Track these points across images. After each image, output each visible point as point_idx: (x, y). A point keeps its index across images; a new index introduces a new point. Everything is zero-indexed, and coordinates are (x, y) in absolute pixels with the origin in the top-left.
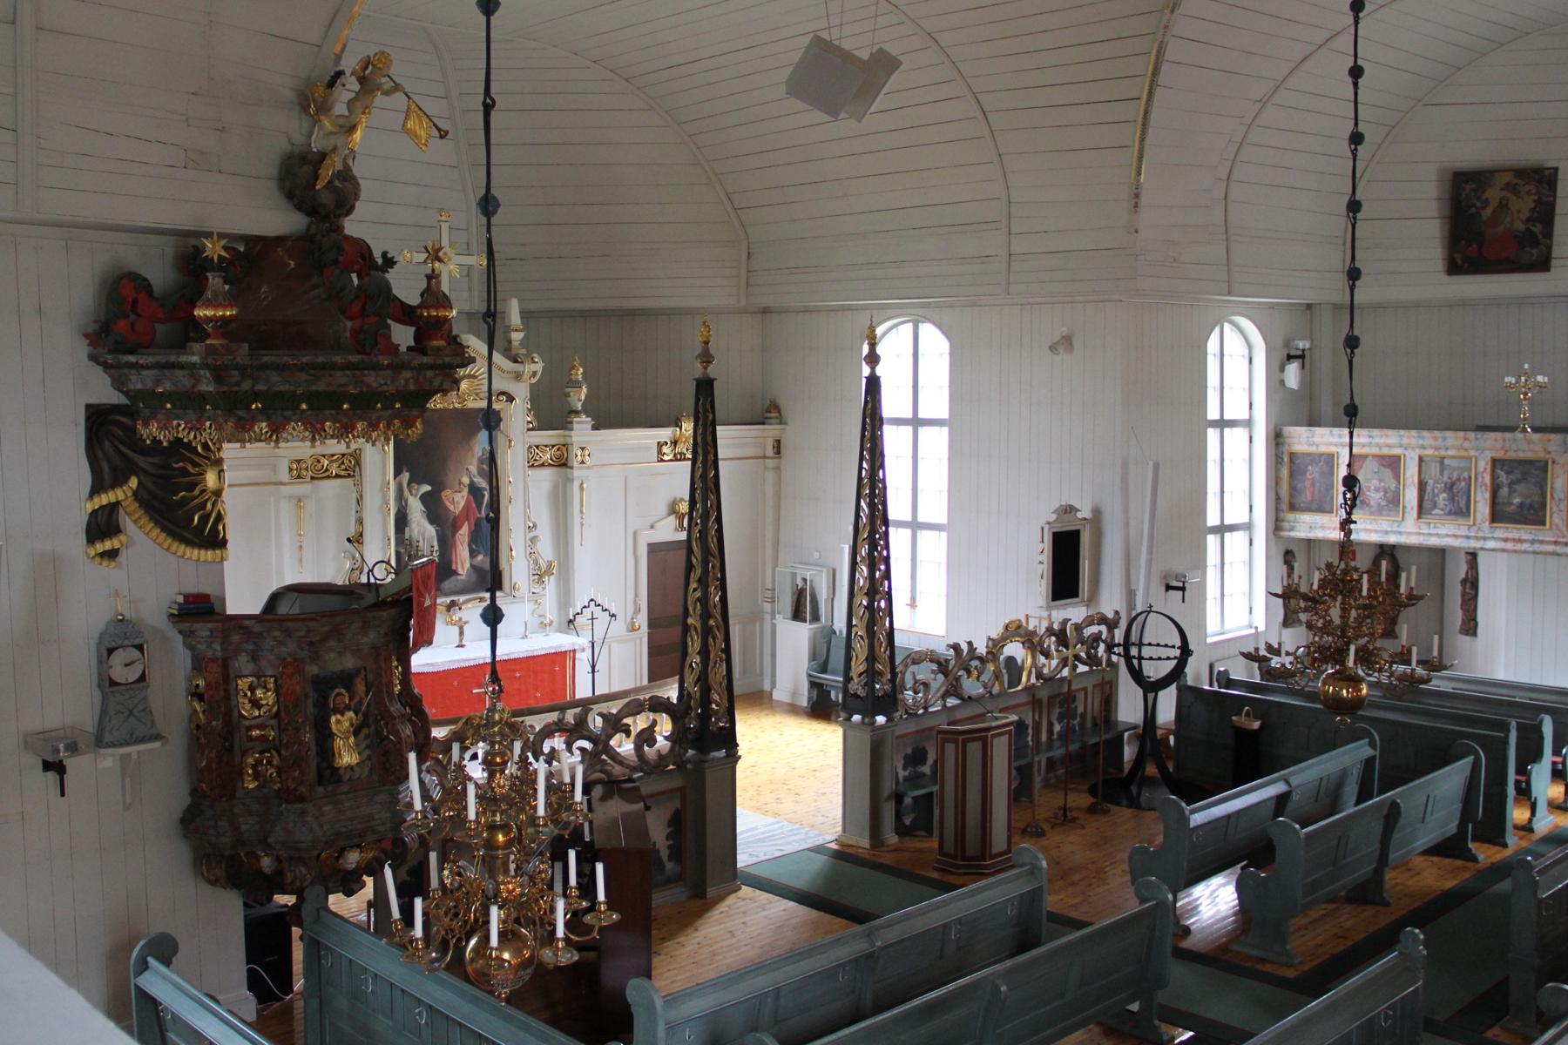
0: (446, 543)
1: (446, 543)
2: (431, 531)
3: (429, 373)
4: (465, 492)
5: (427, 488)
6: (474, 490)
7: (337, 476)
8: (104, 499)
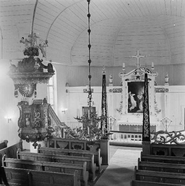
0: (138, 104)
1: (138, 104)
2: (135, 102)
3: (34, 75)
4: (142, 95)
5: (134, 95)
6: (144, 95)
7: (119, 92)
8: (16, 90)
